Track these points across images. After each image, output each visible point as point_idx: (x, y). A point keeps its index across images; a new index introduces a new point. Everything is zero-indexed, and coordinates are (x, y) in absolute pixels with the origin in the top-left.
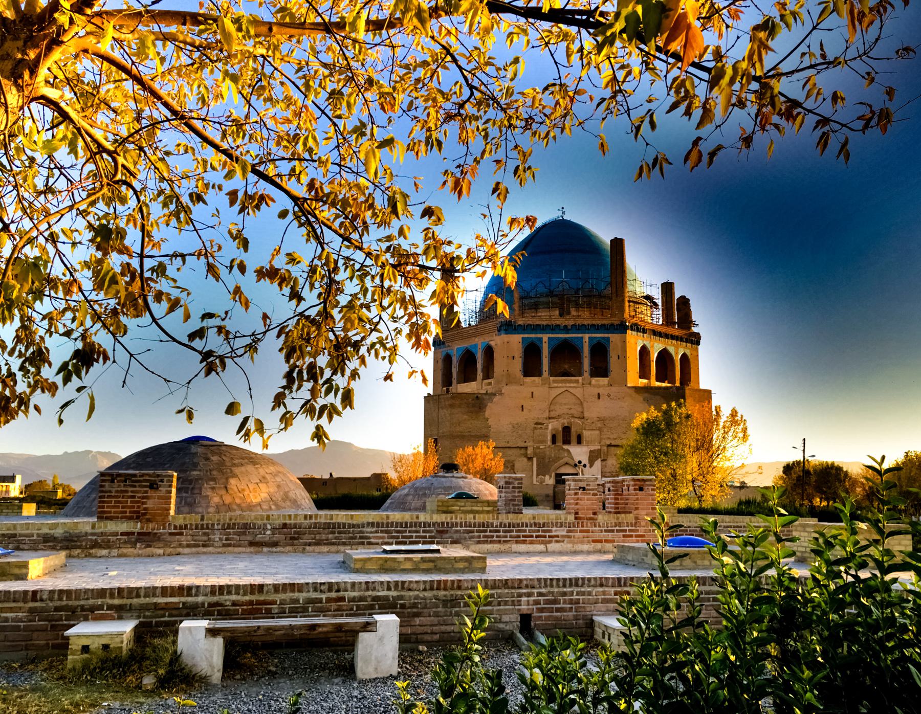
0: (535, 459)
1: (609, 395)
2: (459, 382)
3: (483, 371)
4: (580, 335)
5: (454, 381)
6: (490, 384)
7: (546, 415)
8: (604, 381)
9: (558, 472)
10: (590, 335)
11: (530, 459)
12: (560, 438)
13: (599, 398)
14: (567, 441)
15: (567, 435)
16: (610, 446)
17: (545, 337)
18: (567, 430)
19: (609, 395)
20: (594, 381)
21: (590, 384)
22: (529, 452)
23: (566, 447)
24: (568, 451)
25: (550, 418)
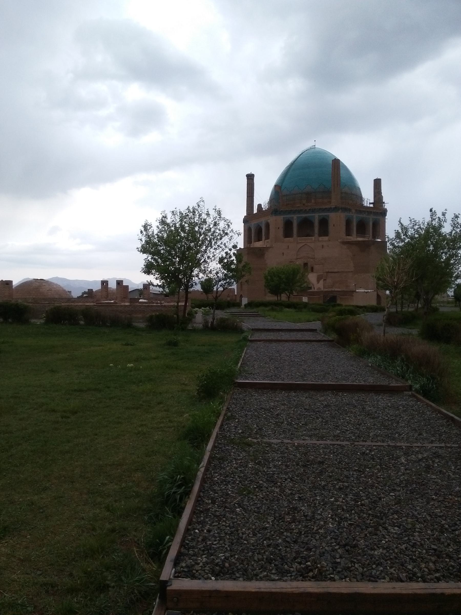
1: (328, 246)
2: (255, 241)
4: (313, 215)
5: (253, 240)
6: (268, 242)
8: (326, 238)
13: (323, 248)
19: (328, 246)
20: (321, 238)
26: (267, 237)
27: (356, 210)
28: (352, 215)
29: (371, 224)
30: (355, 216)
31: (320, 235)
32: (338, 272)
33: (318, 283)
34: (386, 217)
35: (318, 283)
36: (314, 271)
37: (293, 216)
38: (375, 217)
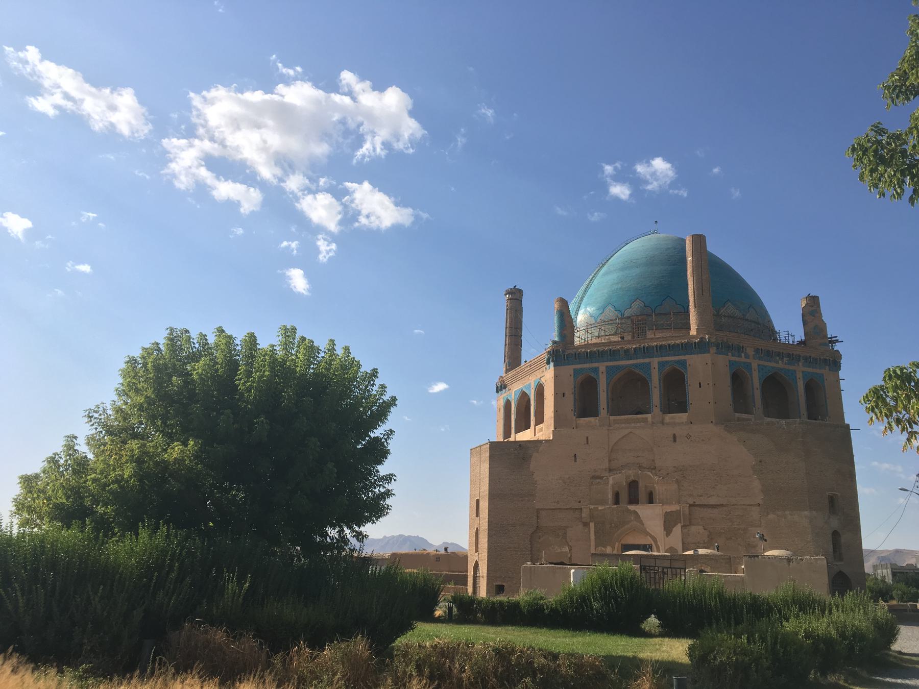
0: (592, 525)
2: (517, 431)
3: (535, 415)
4: (647, 360)
5: (513, 431)
6: (541, 430)
7: (606, 465)
8: (683, 417)
9: (624, 542)
10: (660, 359)
11: (586, 525)
12: (624, 496)
14: (634, 500)
15: (633, 493)
16: (691, 506)
17: (602, 367)
18: (633, 485)
19: (689, 437)
20: (668, 417)
21: (663, 423)
22: (583, 515)
23: (632, 507)
24: (635, 512)
25: (610, 470)
26: (540, 420)
27: (757, 351)
28: (748, 360)
29: (801, 385)
30: (755, 365)
31: (668, 408)
32: (722, 505)
33: (668, 534)
34: (842, 374)
35: (668, 534)
36: (656, 497)
37: (595, 365)
38: (810, 370)
